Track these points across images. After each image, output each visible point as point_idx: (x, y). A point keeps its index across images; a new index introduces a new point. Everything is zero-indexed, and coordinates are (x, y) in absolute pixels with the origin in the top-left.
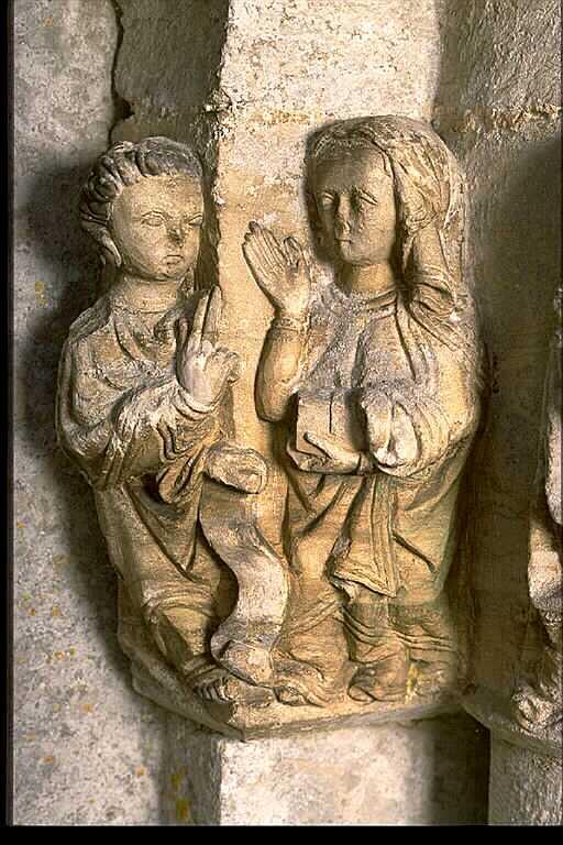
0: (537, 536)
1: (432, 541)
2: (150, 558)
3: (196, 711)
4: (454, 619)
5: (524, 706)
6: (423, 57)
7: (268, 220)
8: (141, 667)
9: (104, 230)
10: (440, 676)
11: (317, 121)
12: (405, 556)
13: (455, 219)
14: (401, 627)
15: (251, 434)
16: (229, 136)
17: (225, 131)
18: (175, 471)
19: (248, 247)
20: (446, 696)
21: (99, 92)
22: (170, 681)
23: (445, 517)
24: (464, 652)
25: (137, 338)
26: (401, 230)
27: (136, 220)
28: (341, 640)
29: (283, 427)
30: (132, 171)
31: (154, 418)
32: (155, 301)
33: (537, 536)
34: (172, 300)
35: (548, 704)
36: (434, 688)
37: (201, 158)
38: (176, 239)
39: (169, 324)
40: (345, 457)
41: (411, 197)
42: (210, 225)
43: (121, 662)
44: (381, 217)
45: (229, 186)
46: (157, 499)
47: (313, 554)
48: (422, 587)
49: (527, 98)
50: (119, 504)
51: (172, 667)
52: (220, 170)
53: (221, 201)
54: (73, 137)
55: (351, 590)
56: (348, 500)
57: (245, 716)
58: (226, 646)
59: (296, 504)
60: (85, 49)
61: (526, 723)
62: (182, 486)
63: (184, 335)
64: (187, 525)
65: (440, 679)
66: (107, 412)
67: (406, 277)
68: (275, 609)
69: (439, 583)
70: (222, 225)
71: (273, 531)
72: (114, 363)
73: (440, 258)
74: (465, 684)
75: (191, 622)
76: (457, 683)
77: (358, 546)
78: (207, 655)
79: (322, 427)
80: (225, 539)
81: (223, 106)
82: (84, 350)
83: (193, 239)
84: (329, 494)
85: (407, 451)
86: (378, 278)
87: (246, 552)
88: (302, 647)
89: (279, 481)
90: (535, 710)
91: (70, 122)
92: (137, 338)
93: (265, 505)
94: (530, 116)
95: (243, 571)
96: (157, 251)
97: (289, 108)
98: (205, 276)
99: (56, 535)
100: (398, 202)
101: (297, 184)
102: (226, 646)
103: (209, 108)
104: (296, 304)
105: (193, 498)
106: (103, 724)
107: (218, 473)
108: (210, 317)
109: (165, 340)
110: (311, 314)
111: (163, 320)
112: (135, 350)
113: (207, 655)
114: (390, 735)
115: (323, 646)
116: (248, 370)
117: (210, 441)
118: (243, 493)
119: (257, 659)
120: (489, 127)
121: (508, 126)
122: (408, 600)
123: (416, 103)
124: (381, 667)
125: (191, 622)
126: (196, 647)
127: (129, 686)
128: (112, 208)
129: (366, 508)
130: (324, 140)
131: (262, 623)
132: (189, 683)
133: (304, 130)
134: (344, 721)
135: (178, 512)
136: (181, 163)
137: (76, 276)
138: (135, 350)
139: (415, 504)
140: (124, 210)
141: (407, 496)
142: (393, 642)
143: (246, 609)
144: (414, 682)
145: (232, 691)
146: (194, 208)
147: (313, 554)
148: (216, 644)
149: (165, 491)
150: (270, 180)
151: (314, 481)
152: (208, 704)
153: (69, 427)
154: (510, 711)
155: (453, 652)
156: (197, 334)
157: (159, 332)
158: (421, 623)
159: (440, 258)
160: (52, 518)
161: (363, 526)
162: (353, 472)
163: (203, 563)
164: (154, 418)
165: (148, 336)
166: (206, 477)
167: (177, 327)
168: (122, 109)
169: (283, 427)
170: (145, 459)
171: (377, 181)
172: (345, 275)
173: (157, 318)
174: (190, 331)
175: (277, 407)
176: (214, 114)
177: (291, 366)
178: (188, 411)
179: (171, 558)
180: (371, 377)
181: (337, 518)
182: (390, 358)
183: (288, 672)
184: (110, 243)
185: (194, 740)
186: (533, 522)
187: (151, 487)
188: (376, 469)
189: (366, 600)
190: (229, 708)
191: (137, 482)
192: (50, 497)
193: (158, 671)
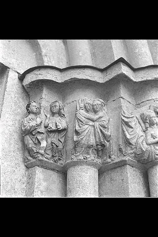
87: (42, 139)
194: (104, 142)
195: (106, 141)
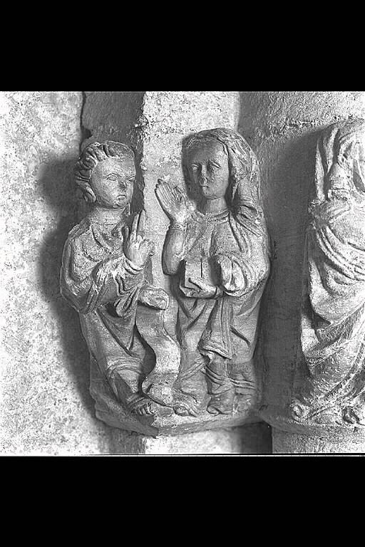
0: (304, 321)
1: (249, 332)
2: (110, 345)
3: (132, 423)
4: (256, 373)
5: (296, 409)
6: (232, 105)
7: (166, 179)
8: (104, 405)
9: (87, 184)
10: (248, 402)
11: (186, 133)
12: (236, 338)
13: (255, 177)
14: (232, 376)
15: (160, 281)
16: (147, 138)
17: (146, 135)
18: (123, 301)
19: (158, 191)
20: (251, 412)
21: (74, 126)
22: (119, 409)
23: (254, 319)
24: (260, 388)
25: (104, 236)
26: (232, 180)
27: (104, 178)
28: (204, 383)
29: (176, 277)
30: (102, 154)
31: (114, 274)
32: (109, 219)
33: (304, 321)
34: (119, 218)
35: (308, 408)
36: (246, 408)
37: (133, 149)
38: (123, 187)
39: (119, 229)
40: (209, 289)
41: (237, 164)
42: (139, 181)
43: (89, 403)
44: (222, 174)
45: (147, 161)
46: (116, 316)
47: (192, 340)
48: (242, 354)
49: (287, 119)
50: (94, 321)
51: (119, 401)
52: (144, 154)
53: (145, 169)
54: (63, 147)
55: (211, 356)
56: (209, 311)
57: (161, 421)
58: (150, 387)
59: (183, 315)
60: (67, 105)
61: (297, 418)
62: (128, 307)
63: (127, 233)
64: (130, 327)
65: (249, 403)
66: (90, 272)
67: (233, 203)
68: (174, 366)
69: (251, 353)
70: (146, 180)
71: (172, 328)
72: (93, 249)
73: (250, 193)
74: (261, 405)
75: (131, 377)
76: (256, 405)
77: (215, 333)
78: (140, 393)
79: (197, 275)
80: (148, 332)
81: (144, 124)
82: (78, 243)
83: (130, 187)
84: (199, 309)
85: (240, 283)
86: (219, 205)
87: (160, 338)
88: (186, 386)
89: (174, 304)
90: (302, 411)
91: (61, 139)
92: (104, 236)
93: (168, 317)
94: (288, 127)
95: (158, 349)
96: (114, 193)
97: (174, 126)
98: (137, 205)
99: (58, 341)
100: (230, 166)
101: (179, 162)
102: (150, 387)
103: (136, 126)
104: (181, 218)
105: (132, 313)
106: (81, 436)
107: (146, 300)
108: (140, 224)
109: (118, 236)
110: (187, 223)
111: (116, 228)
112: (103, 242)
113: (140, 393)
114: (221, 434)
115: (195, 385)
116: (158, 250)
117: (140, 285)
118: (158, 309)
119: (165, 392)
120: (268, 134)
121: (278, 133)
122: (237, 361)
123: (231, 123)
124: (223, 396)
125: (131, 377)
126: (134, 389)
127: (94, 416)
128: (91, 173)
129: (218, 315)
130: (192, 141)
131: (169, 373)
132: (131, 410)
133: (181, 137)
134: (203, 427)
135: (125, 321)
136: (124, 151)
137: (65, 214)
138: (103, 242)
139: (241, 312)
140: (98, 173)
141: (237, 308)
142: (228, 383)
143: (159, 368)
144: (236, 405)
145: (154, 409)
146: (131, 172)
147: (192, 340)
148: (144, 386)
149: (118, 312)
150: (167, 160)
151: (192, 303)
152: (139, 417)
153: (69, 282)
154: (288, 412)
155: (254, 390)
156: (135, 233)
157: (114, 233)
158: (242, 373)
159: (250, 193)
160: (56, 332)
161: (217, 323)
162: (212, 297)
163: (137, 346)
164: (114, 274)
165: (109, 235)
166: (140, 303)
167: (123, 230)
168: (86, 133)
169: (176, 277)
170: (108, 295)
171: (220, 157)
172: (202, 203)
173: (113, 227)
174: (130, 232)
175: (173, 266)
176: (140, 128)
177: (180, 246)
178: (131, 270)
179: (122, 345)
180: (220, 250)
181: (204, 320)
182: (228, 241)
183: (180, 399)
184: (90, 190)
185: (128, 440)
186: (302, 315)
187: (111, 309)
188: (225, 294)
189: (218, 361)
190: (152, 417)
191: (103, 308)
192: (55, 322)
193: (111, 405)
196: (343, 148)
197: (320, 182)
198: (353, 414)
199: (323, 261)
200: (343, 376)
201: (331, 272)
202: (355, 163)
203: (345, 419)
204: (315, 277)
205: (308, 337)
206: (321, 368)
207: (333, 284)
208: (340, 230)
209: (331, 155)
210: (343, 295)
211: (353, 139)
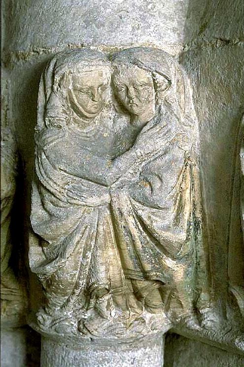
0: (32, 240)
5: (40, 318)
24: (25, 295)
35: (50, 317)
36: (14, 312)
49: (31, 46)
61: (41, 326)
65: (17, 308)
76: (24, 309)
90: (44, 320)
94: (32, 53)
120: (18, 60)
121: (25, 58)
144: (5, 310)
154: (37, 322)
155: (21, 296)
186: (30, 234)
194: (162, 268)
195: (169, 262)
196: (57, 78)
197: (40, 109)
198: (84, 326)
199: (40, 185)
200: (69, 291)
201: (47, 195)
202: (69, 92)
203: (79, 330)
204: (35, 199)
205: (35, 255)
206: (51, 281)
207: (50, 206)
208: (52, 156)
209: (49, 84)
210: (59, 218)
211: (65, 69)
